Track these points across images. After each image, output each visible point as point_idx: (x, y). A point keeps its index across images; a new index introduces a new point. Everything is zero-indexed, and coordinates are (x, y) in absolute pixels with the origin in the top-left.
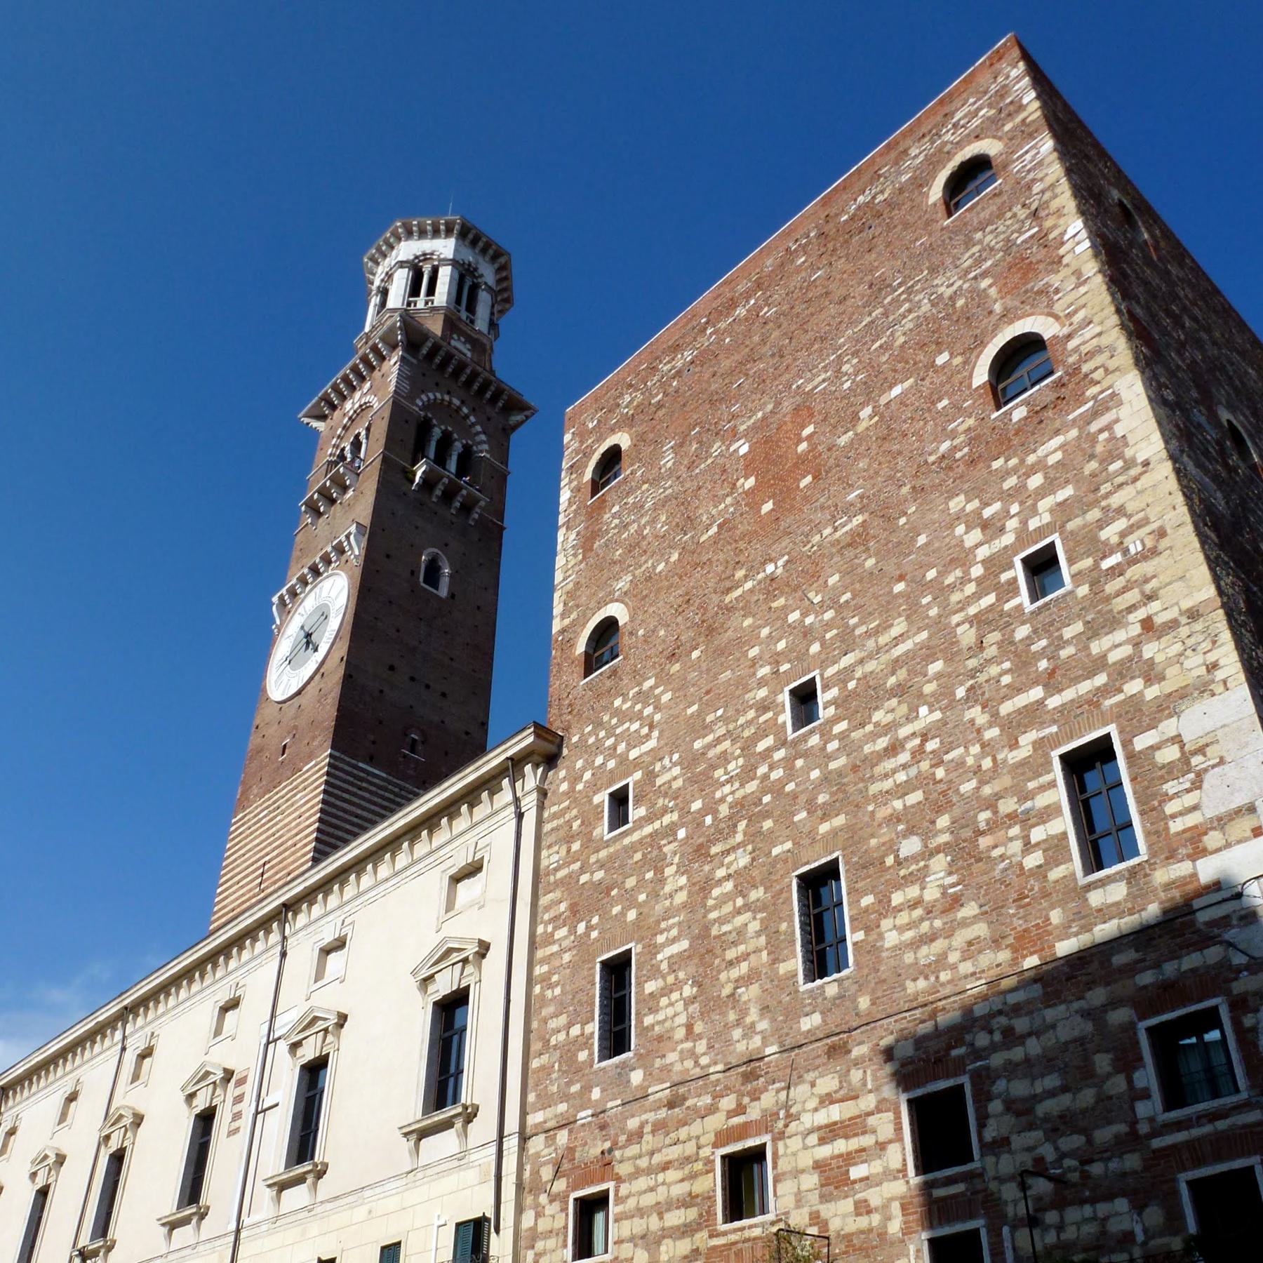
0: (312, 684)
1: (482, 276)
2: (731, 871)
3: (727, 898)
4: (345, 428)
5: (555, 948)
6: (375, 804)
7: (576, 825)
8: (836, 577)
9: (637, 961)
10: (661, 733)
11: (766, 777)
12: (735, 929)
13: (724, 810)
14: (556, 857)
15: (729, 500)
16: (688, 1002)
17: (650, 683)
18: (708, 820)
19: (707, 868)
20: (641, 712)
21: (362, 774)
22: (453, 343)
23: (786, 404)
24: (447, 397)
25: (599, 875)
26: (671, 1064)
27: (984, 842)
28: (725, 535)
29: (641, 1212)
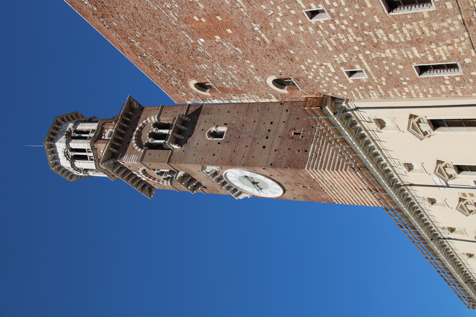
0: (275, 179)
1: (70, 129)
2: (383, 34)
3: (396, 36)
4: (154, 179)
5: (413, 92)
7: (361, 88)
8: (263, 6)
9: (420, 64)
10: (324, 62)
11: (346, 26)
12: (409, 32)
13: (359, 39)
14: (375, 94)
15: (224, 44)
16: (438, 45)
17: (303, 67)
18: (362, 44)
19: (383, 43)
20: (315, 69)
22: (106, 138)
23: (183, 27)
24: (134, 138)
25: (383, 79)
26: (463, 50)
28: (240, 45)
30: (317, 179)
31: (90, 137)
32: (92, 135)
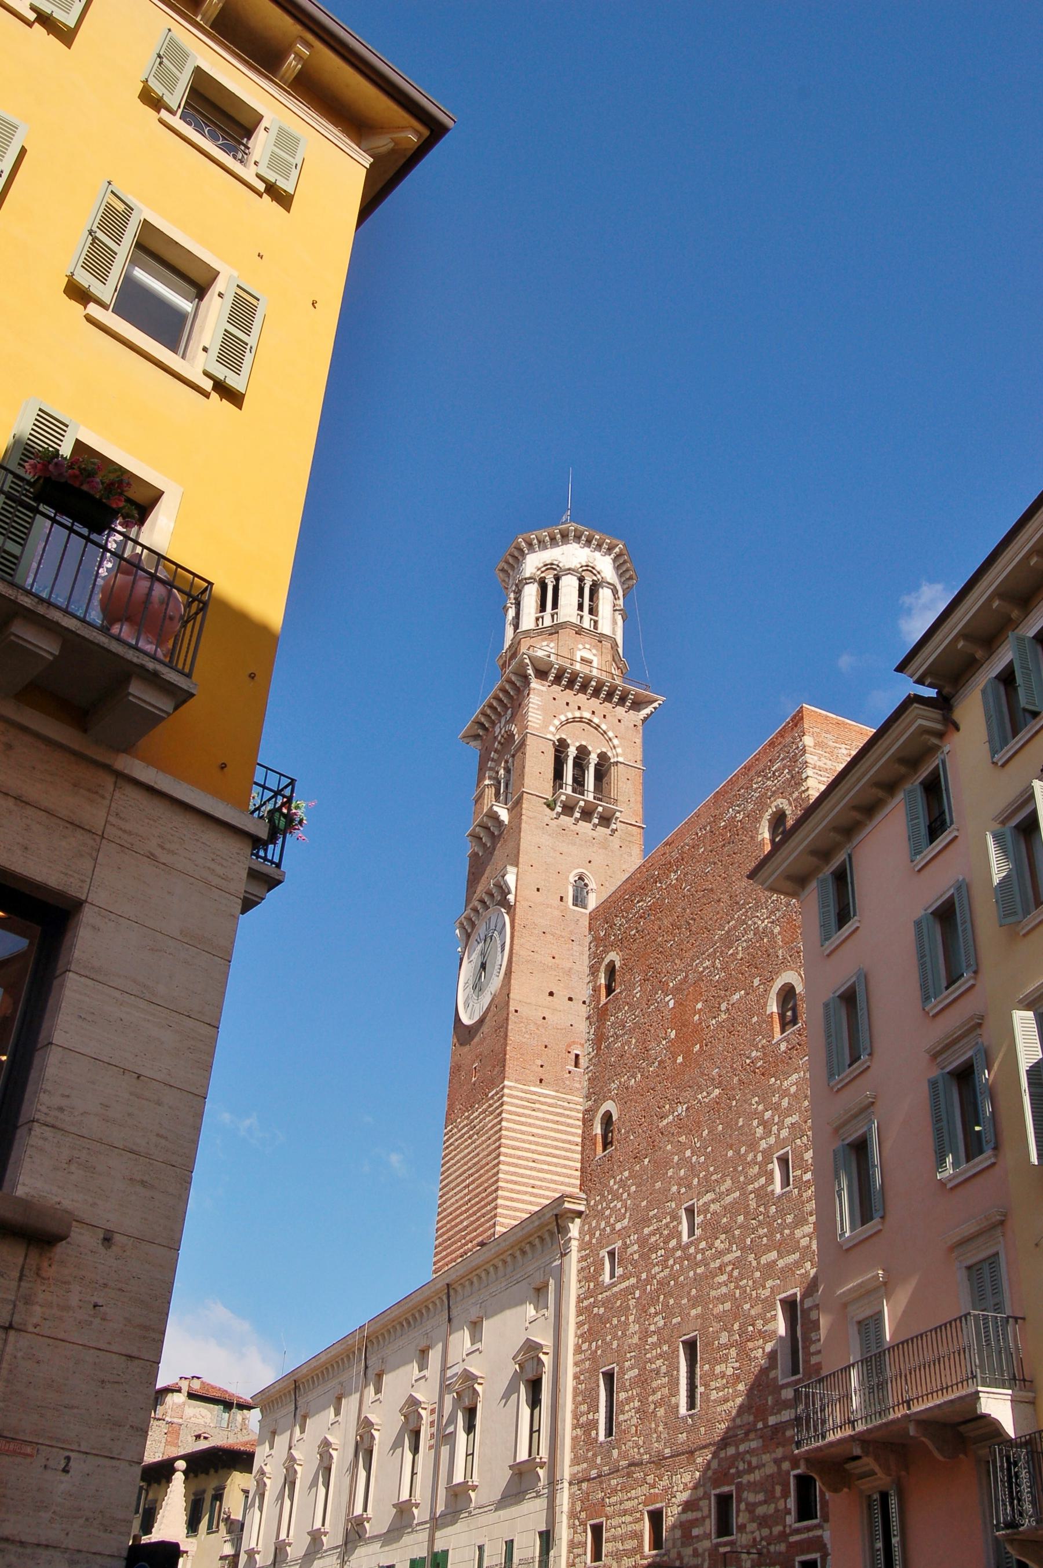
3: (654, 1346)
6: (547, 1121)
21: (534, 1097)
27: (750, 1345)
29: (614, 1539)
31: (582, 617)
32: (587, 623)
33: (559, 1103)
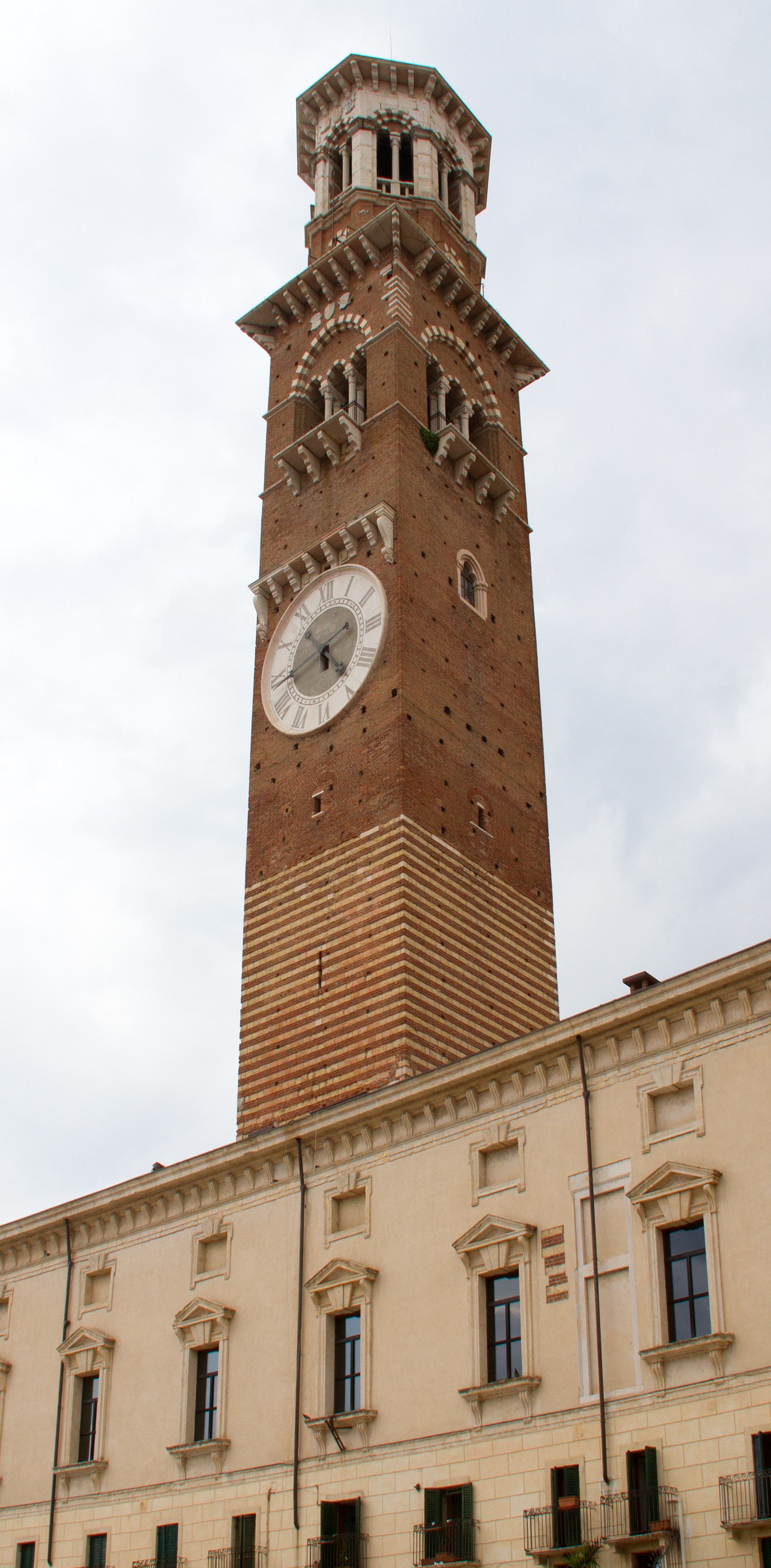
6: (454, 890)
30: (356, 844)
33: (465, 869)
